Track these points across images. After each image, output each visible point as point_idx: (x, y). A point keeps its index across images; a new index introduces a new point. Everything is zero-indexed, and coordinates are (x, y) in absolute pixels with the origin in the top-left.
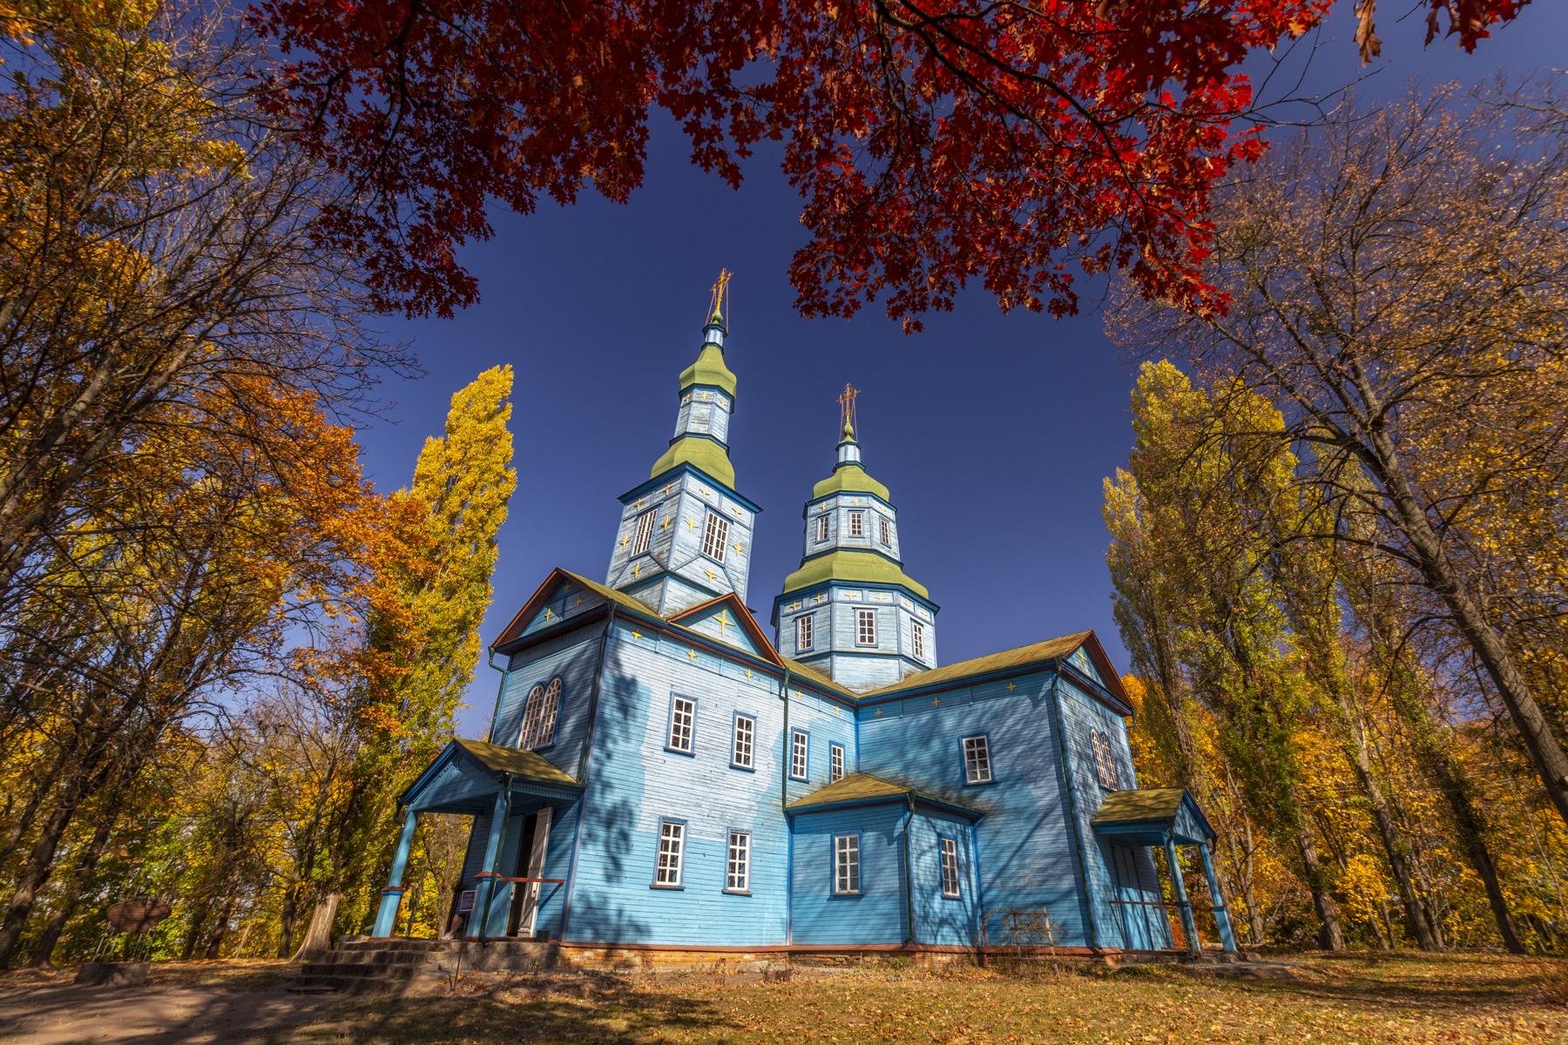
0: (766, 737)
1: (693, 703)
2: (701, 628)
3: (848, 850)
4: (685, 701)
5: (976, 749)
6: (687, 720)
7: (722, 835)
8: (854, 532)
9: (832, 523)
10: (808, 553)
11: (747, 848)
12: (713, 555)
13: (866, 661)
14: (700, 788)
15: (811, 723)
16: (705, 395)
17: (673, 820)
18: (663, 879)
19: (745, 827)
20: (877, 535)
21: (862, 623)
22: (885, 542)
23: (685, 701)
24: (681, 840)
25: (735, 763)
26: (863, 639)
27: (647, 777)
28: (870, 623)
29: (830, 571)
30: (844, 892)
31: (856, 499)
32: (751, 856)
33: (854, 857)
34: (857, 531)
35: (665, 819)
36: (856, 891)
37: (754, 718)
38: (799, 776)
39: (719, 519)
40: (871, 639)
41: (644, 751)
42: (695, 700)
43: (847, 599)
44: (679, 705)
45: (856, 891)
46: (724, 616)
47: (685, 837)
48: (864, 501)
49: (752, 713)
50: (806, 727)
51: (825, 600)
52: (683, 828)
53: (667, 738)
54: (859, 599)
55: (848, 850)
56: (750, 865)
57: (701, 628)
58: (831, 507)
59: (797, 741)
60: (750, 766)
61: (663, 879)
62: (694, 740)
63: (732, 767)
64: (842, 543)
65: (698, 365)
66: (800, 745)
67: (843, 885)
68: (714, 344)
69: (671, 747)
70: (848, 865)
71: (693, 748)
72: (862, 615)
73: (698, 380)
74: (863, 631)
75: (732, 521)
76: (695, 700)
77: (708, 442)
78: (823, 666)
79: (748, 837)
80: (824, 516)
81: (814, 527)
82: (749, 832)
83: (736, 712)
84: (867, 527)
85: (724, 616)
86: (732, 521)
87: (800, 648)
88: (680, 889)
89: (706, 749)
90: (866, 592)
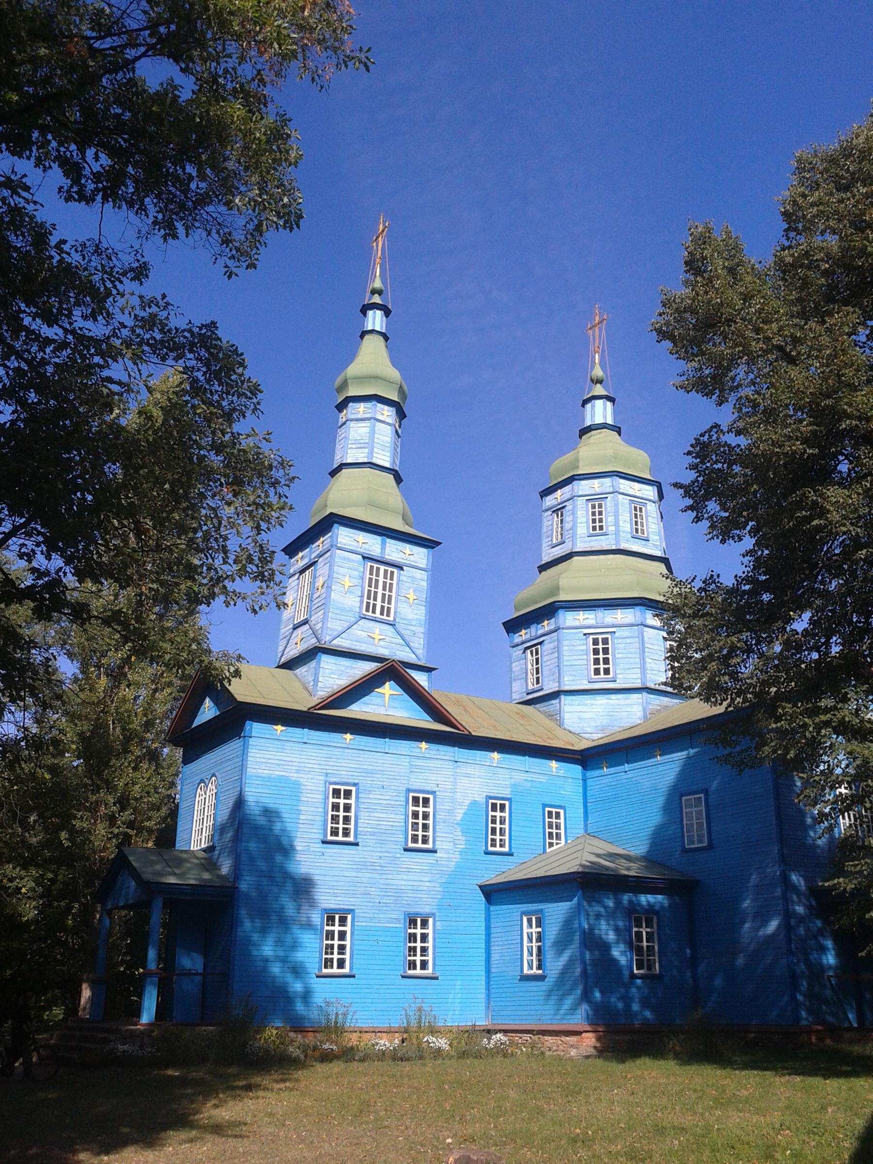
0: (451, 812)
1: (353, 789)
2: (359, 710)
6: (347, 808)
7: (397, 920)
9: (568, 518)
10: (546, 559)
11: (430, 931)
12: (378, 614)
13: (601, 700)
14: (368, 875)
15: (514, 786)
16: (361, 409)
17: (337, 911)
19: (426, 910)
20: (626, 526)
21: (596, 652)
22: (638, 534)
26: (597, 672)
28: (606, 651)
29: (556, 590)
30: (531, 972)
32: (434, 939)
34: (597, 527)
36: (540, 972)
37: (433, 793)
38: (498, 849)
39: (382, 568)
40: (607, 671)
42: (355, 785)
43: (577, 623)
44: (336, 793)
46: (389, 689)
50: (507, 793)
51: (552, 627)
52: (349, 917)
53: (325, 830)
54: (591, 622)
56: (434, 947)
57: (359, 710)
58: (568, 496)
60: (430, 846)
64: (580, 547)
65: (352, 370)
66: (498, 814)
68: (372, 331)
69: (330, 838)
71: (356, 836)
72: (595, 642)
73: (352, 392)
74: (596, 661)
76: (355, 785)
77: (367, 471)
78: (552, 708)
79: (431, 921)
80: (558, 510)
81: (550, 522)
82: (433, 915)
83: (409, 791)
84: (611, 519)
85: (389, 689)
87: (530, 687)
89: (373, 834)
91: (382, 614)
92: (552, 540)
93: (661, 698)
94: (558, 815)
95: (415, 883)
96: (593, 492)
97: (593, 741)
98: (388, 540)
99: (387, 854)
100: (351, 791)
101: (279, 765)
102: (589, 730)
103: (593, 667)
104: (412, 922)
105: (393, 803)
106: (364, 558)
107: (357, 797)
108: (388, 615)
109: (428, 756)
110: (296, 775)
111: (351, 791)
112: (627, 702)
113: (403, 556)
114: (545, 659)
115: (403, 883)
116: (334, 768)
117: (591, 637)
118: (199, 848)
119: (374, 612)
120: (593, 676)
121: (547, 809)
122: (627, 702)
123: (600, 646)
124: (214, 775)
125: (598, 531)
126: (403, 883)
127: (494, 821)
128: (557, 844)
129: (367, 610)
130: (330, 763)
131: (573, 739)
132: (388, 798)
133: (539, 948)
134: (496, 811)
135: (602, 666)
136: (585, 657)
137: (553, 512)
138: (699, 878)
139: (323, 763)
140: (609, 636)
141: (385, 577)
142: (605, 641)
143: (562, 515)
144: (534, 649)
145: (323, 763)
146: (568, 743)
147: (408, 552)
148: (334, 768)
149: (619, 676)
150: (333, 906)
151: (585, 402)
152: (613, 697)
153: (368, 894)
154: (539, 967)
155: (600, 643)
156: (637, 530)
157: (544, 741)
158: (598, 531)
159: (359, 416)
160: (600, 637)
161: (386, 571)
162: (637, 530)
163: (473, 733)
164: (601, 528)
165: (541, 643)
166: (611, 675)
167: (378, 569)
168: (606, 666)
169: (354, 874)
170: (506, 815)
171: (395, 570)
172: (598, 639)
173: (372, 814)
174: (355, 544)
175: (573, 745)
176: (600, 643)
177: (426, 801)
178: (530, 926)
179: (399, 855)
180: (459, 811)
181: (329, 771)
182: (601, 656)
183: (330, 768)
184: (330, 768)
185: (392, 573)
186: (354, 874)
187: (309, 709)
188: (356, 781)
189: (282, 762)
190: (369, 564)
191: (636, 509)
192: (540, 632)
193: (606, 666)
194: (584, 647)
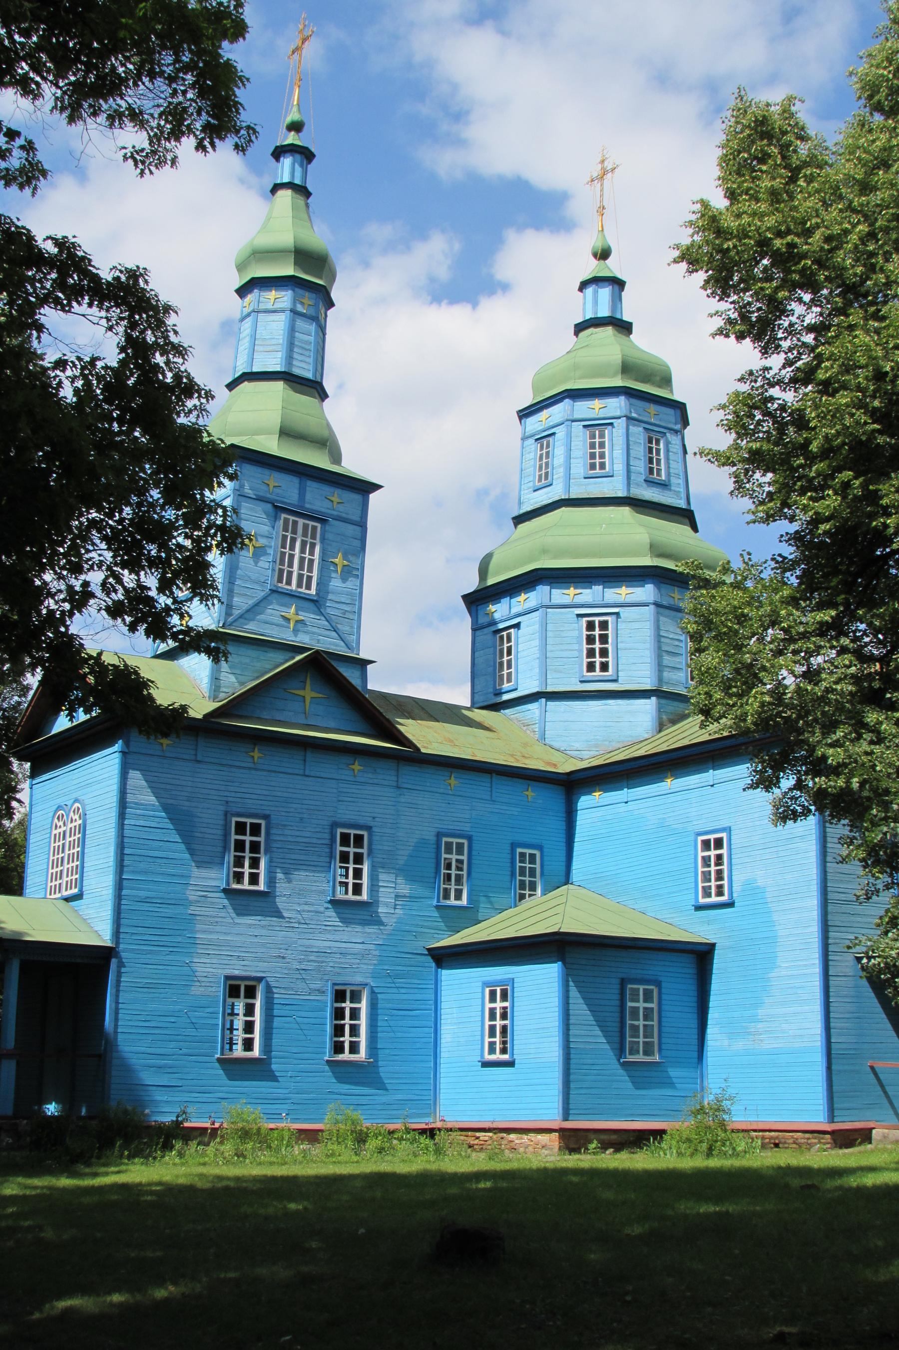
5: (713, 853)
8: (593, 467)
12: (294, 586)
19: (359, 979)
21: (590, 640)
26: (591, 667)
28: (604, 639)
30: (493, 1057)
31: (597, 403)
37: (369, 828)
39: (301, 522)
40: (604, 667)
41: (192, 895)
42: (266, 817)
43: (566, 600)
44: (241, 828)
45: (506, 1057)
46: (309, 693)
48: (616, 405)
49: (362, 821)
50: (466, 828)
59: (449, 850)
72: (590, 626)
83: (335, 825)
90: (598, 589)
91: (299, 585)
92: (534, 481)
93: (676, 704)
94: (532, 858)
95: (344, 945)
97: (582, 760)
98: (309, 483)
99: (306, 908)
100: (259, 825)
101: (165, 790)
102: (577, 745)
103: (586, 661)
104: (340, 996)
105: (314, 841)
106: (276, 507)
107: (268, 834)
108: (308, 587)
109: (362, 780)
110: (187, 803)
111: (259, 825)
113: (329, 505)
116: (239, 795)
118: (58, 895)
119: (289, 583)
120: (585, 673)
121: (519, 850)
123: (597, 632)
124: (76, 801)
125: (598, 471)
127: (448, 867)
128: (530, 895)
129: (280, 580)
130: (232, 789)
131: (556, 757)
132: (308, 834)
133: (504, 1029)
134: (451, 853)
135: (598, 660)
137: (536, 440)
138: (713, 941)
139: (223, 788)
140: (608, 618)
141: (305, 534)
142: (604, 625)
143: (548, 446)
144: (505, 633)
145: (223, 788)
146: (549, 764)
147: (335, 499)
148: (239, 795)
149: (620, 674)
153: (283, 958)
154: (504, 1051)
155: (597, 629)
156: (651, 471)
157: (518, 761)
158: (598, 471)
159: (270, 306)
160: (597, 620)
161: (305, 527)
162: (651, 471)
163: (423, 750)
164: (602, 466)
167: (295, 523)
168: (604, 660)
170: (464, 858)
171: (319, 525)
172: (593, 622)
173: (288, 856)
174: (264, 488)
175: (555, 766)
176: (597, 629)
177: (359, 840)
178: (493, 999)
179: (322, 909)
180: (401, 852)
181: (230, 799)
182: (597, 646)
183: (233, 794)
184: (233, 794)
185: (314, 528)
187: (205, 716)
188: (267, 812)
189: (169, 787)
190: (283, 516)
191: (650, 442)
192: (514, 611)
193: (604, 660)
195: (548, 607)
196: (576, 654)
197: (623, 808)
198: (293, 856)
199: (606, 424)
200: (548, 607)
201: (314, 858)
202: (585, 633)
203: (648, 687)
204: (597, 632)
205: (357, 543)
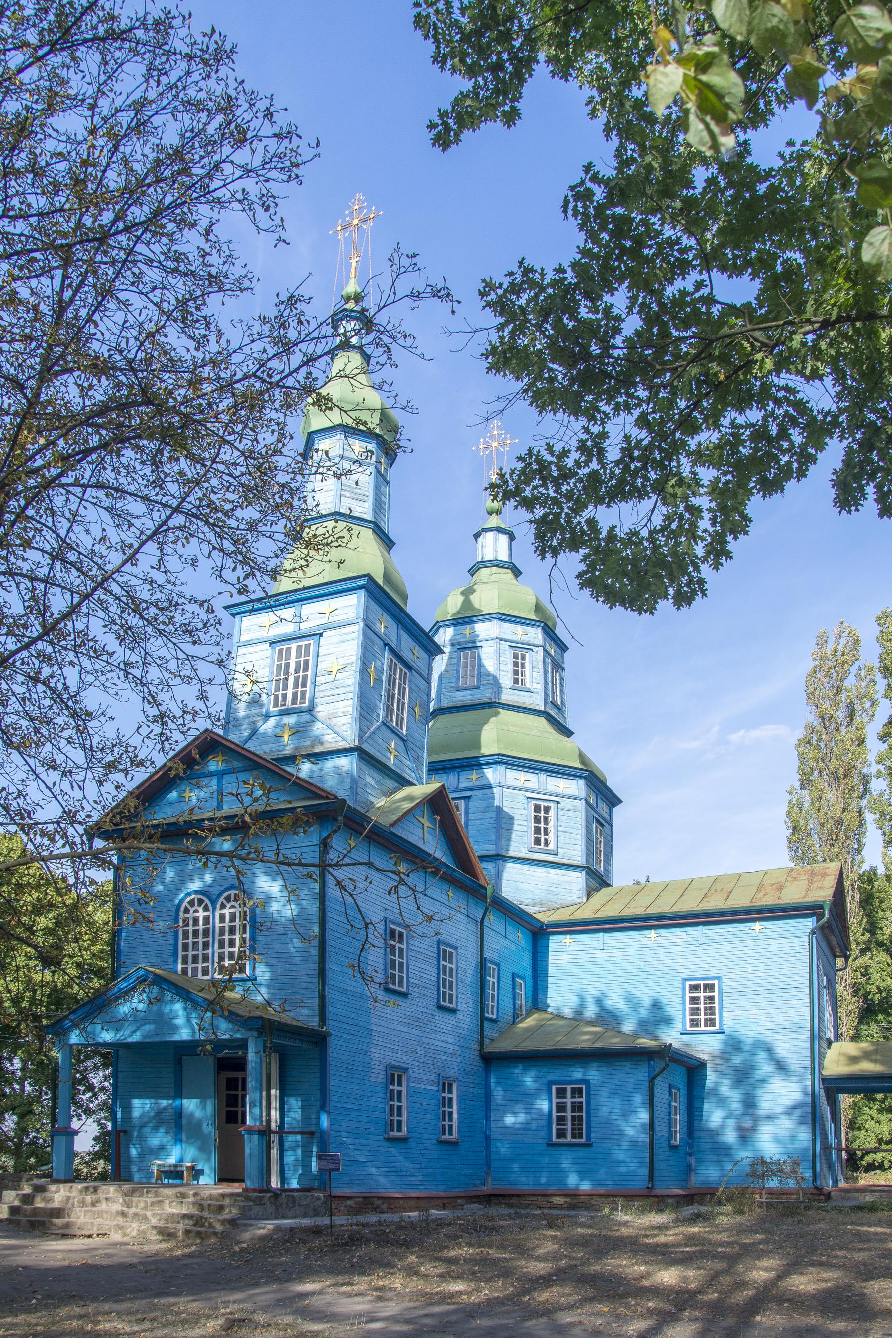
3: (569, 1100)
4: (398, 929)
13: (539, 872)
14: (415, 1032)
18: (392, 1129)
23: (398, 929)
24: (404, 1089)
25: (442, 1003)
26: (537, 841)
27: (373, 1020)
31: (520, 629)
33: (577, 1107)
35: (392, 1067)
37: (456, 948)
39: (399, 665)
40: (546, 843)
47: (408, 1086)
49: (453, 941)
55: (569, 1100)
61: (392, 1129)
62: (408, 977)
63: (441, 1008)
67: (561, 1134)
70: (569, 1114)
71: (408, 986)
72: (537, 809)
75: (410, 668)
86: (410, 668)
88: (404, 1140)
89: (417, 986)
90: (543, 776)
92: (457, 682)
96: (514, 638)
103: (533, 836)
112: (566, 878)
113: (411, 656)
114: (471, 817)
115: (437, 1043)
117: (534, 802)
122: (566, 878)
126: (437, 1043)
136: (525, 823)
150: (394, 1063)
151: (477, 536)
152: (552, 871)
160: (543, 804)
165: (469, 798)
166: (551, 847)
169: (404, 1029)
182: (542, 825)
186: (404, 1029)
192: (463, 785)
194: (526, 812)
195: (503, 787)
196: (525, 829)
197: (597, 955)
198: (420, 965)
199: (529, 647)
200: (503, 787)
201: (429, 968)
202: (533, 813)
203: (579, 864)
204: (542, 814)
205: (425, 697)
